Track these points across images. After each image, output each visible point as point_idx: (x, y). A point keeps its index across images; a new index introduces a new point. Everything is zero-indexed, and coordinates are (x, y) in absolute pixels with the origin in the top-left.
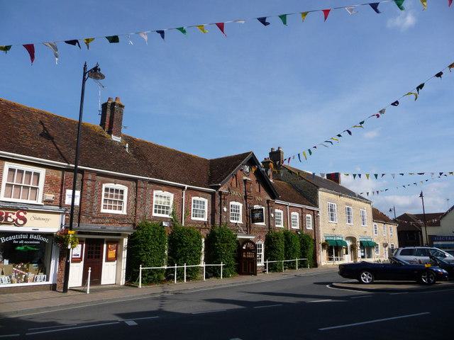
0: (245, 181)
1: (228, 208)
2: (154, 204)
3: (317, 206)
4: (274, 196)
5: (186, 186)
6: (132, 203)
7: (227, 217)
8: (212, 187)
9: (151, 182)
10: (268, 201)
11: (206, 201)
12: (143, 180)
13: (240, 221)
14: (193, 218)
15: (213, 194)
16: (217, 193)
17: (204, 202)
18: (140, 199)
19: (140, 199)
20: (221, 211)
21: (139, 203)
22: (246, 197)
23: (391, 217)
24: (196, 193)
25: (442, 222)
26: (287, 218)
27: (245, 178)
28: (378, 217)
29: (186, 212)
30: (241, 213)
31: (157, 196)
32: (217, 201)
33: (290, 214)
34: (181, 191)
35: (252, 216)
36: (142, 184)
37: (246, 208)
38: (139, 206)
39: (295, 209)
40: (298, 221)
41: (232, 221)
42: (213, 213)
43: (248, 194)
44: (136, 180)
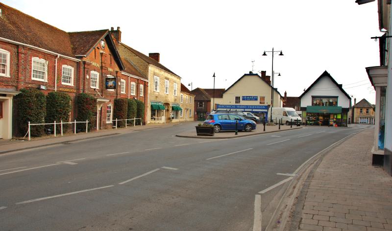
0: (102, 54)
1: (89, 76)
2: (32, 69)
3: (148, 79)
4: (121, 68)
5: (59, 55)
6: (15, 67)
7: (89, 84)
8: (77, 57)
9: (30, 49)
10: (117, 72)
11: (73, 69)
12: (23, 47)
13: (97, 87)
14: (63, 83)
15: (78, 63)
16: (81, 63)
17: (71, 70)
18: (20, 64)
19: (20, 64)
20: (84, 78)
21: (21, 67)
22: (102, 67)
23: (190, 89)
24: (66, 62)
25: (225, 95)
26: (128, 88)
27: (101, 51)
28: (184, 89)
29: (58, 78)
30: (98, 81)
31: (34, 62)
32: (82, 70)
33: (130, 83)
34: (53, 60)
35: (105, 82)
36: (23, 51)
37: (102, 76)
38: (20, 70)
39: (133, 79)
40: (135, 89)
41: (92, 87)
42: (77, 80)
43: (103, 65)
44: (17, 46)
